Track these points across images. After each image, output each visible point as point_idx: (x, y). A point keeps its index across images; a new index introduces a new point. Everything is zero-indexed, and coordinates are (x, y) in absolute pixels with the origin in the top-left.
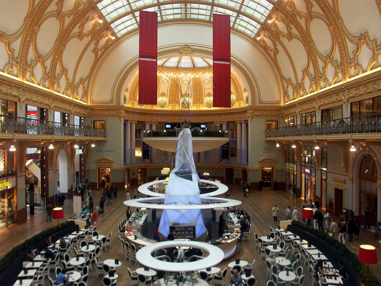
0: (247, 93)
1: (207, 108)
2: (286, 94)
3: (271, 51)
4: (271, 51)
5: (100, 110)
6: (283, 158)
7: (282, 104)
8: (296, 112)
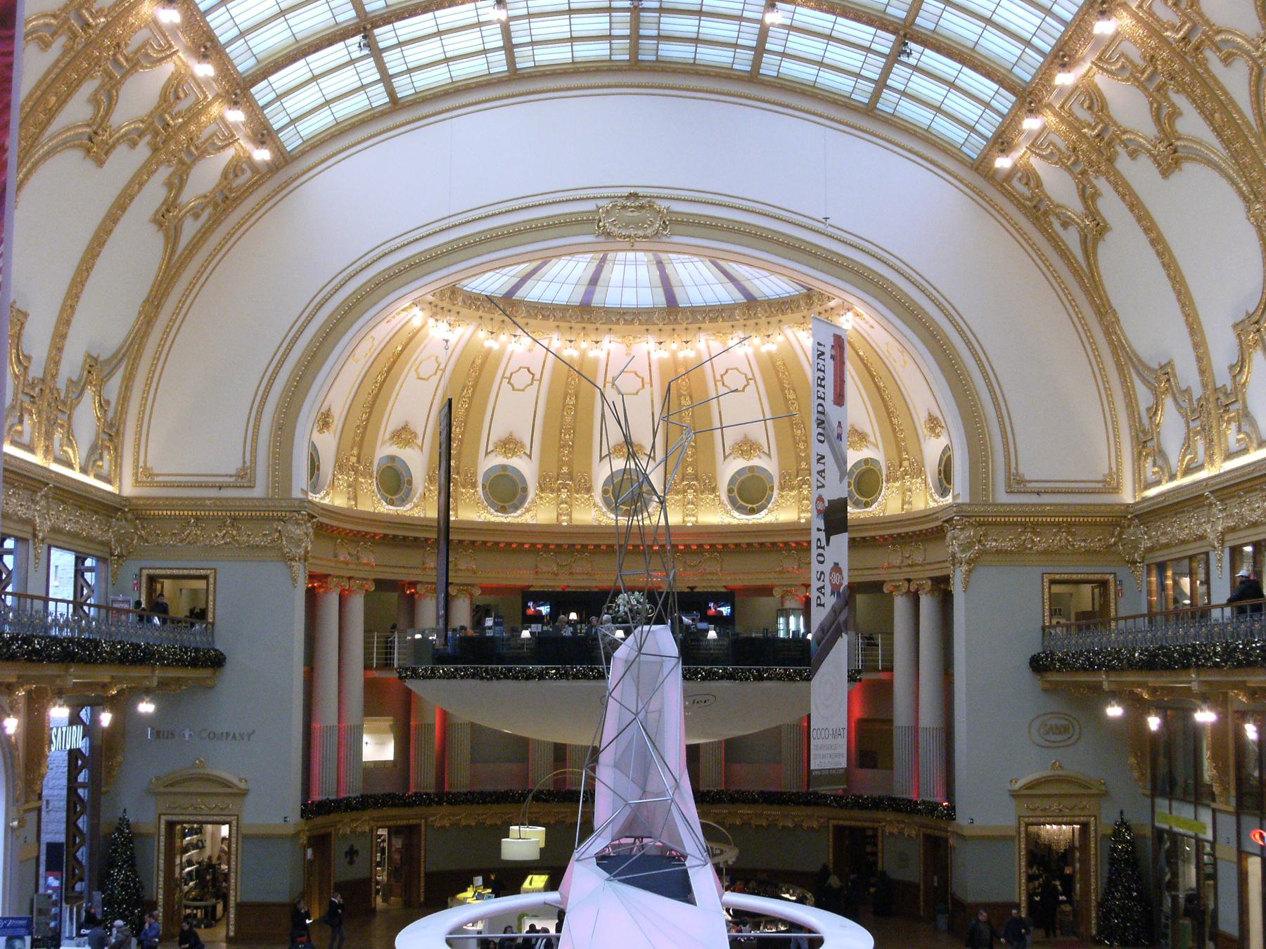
0: (943, 441)
1: (736, 514)
2: (1145, 442)
3: (1065, 225)
4: (1065, 225)
5: (186, 519)
6: (1136, 774)
7: (1128, 496)
8: (1201, 538)
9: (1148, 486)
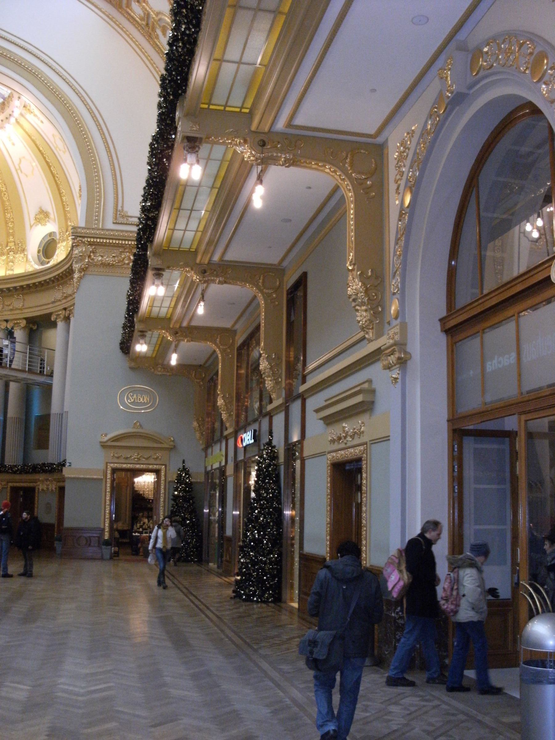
6: (198, 435)
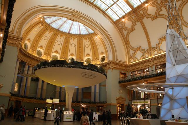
7: (128, 64)
9: (131, 63)
